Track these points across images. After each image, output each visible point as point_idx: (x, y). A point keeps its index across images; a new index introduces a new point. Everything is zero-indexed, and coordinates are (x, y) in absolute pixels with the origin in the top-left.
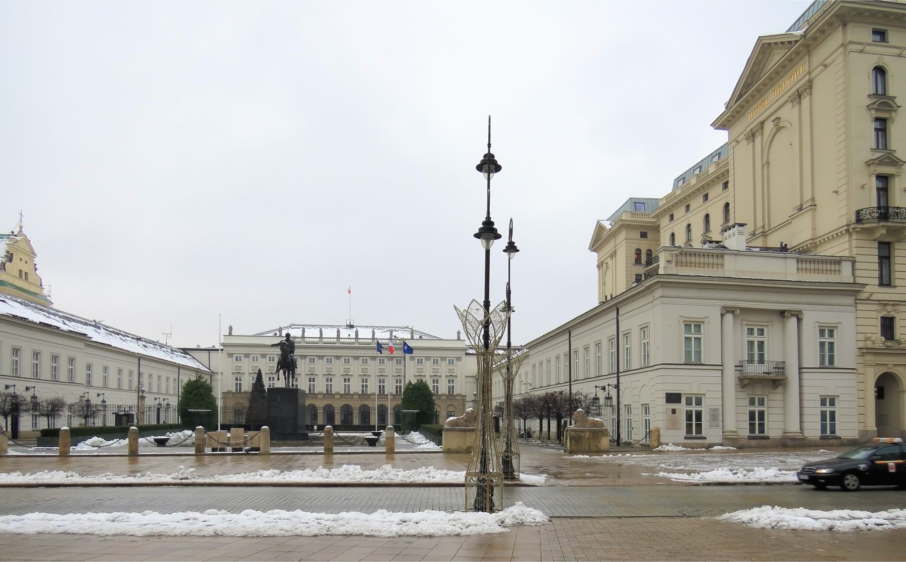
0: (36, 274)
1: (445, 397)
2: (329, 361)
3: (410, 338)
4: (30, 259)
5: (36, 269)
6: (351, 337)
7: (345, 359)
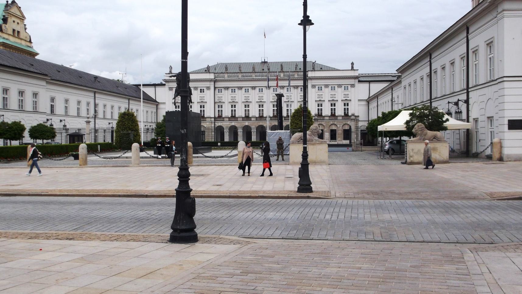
0: (26, 32)
1: (341, 118)
2: (247, 91)
3: (312, 69)
4: (21, 21)
5: (25, 29)
6: (264, 71)
7: (259, 89)
